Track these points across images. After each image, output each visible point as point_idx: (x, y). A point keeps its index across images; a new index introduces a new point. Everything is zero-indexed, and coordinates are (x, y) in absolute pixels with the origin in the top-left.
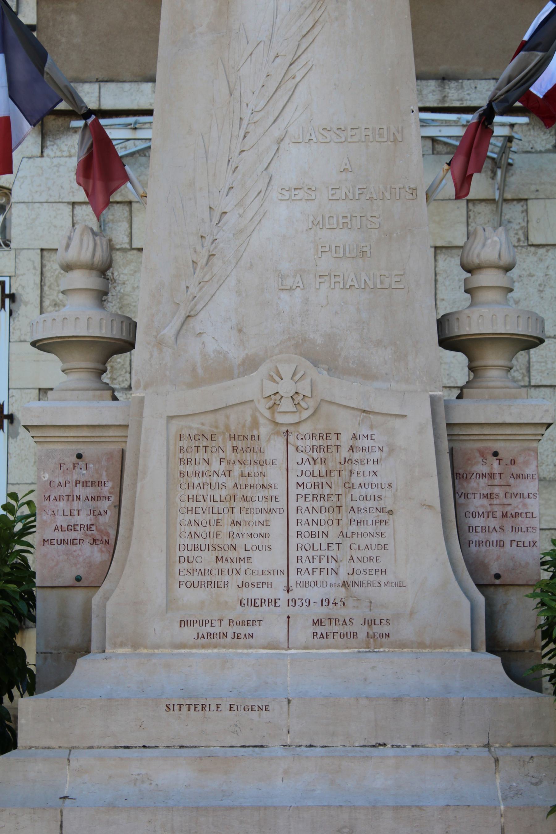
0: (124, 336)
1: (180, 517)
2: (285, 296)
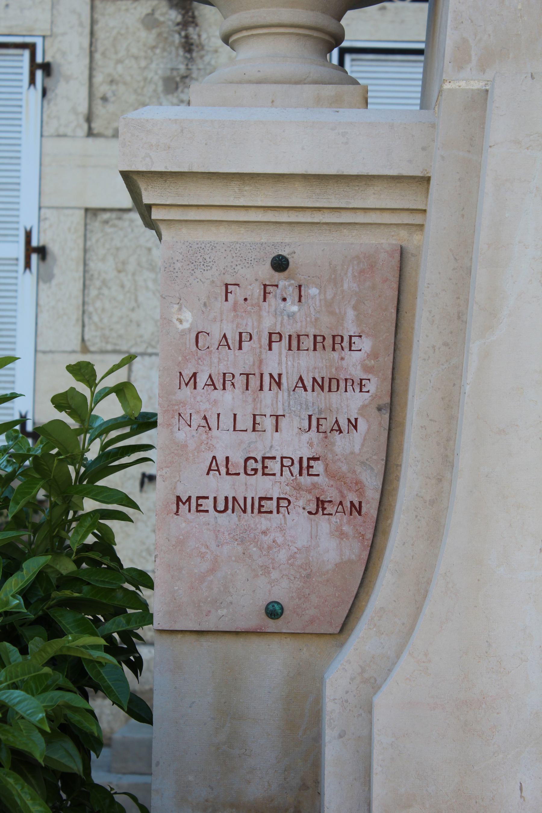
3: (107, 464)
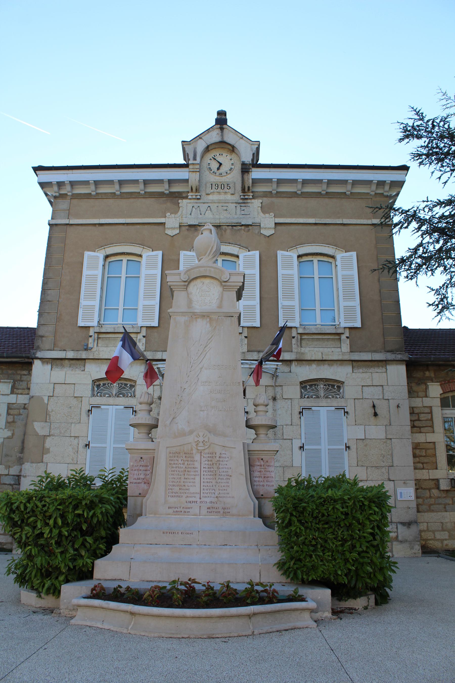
0: (156, 423)
1: (169, 476)
2: (202, 413)
3: (126, 480)
